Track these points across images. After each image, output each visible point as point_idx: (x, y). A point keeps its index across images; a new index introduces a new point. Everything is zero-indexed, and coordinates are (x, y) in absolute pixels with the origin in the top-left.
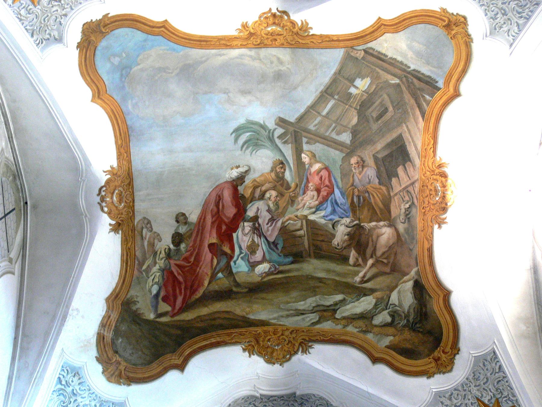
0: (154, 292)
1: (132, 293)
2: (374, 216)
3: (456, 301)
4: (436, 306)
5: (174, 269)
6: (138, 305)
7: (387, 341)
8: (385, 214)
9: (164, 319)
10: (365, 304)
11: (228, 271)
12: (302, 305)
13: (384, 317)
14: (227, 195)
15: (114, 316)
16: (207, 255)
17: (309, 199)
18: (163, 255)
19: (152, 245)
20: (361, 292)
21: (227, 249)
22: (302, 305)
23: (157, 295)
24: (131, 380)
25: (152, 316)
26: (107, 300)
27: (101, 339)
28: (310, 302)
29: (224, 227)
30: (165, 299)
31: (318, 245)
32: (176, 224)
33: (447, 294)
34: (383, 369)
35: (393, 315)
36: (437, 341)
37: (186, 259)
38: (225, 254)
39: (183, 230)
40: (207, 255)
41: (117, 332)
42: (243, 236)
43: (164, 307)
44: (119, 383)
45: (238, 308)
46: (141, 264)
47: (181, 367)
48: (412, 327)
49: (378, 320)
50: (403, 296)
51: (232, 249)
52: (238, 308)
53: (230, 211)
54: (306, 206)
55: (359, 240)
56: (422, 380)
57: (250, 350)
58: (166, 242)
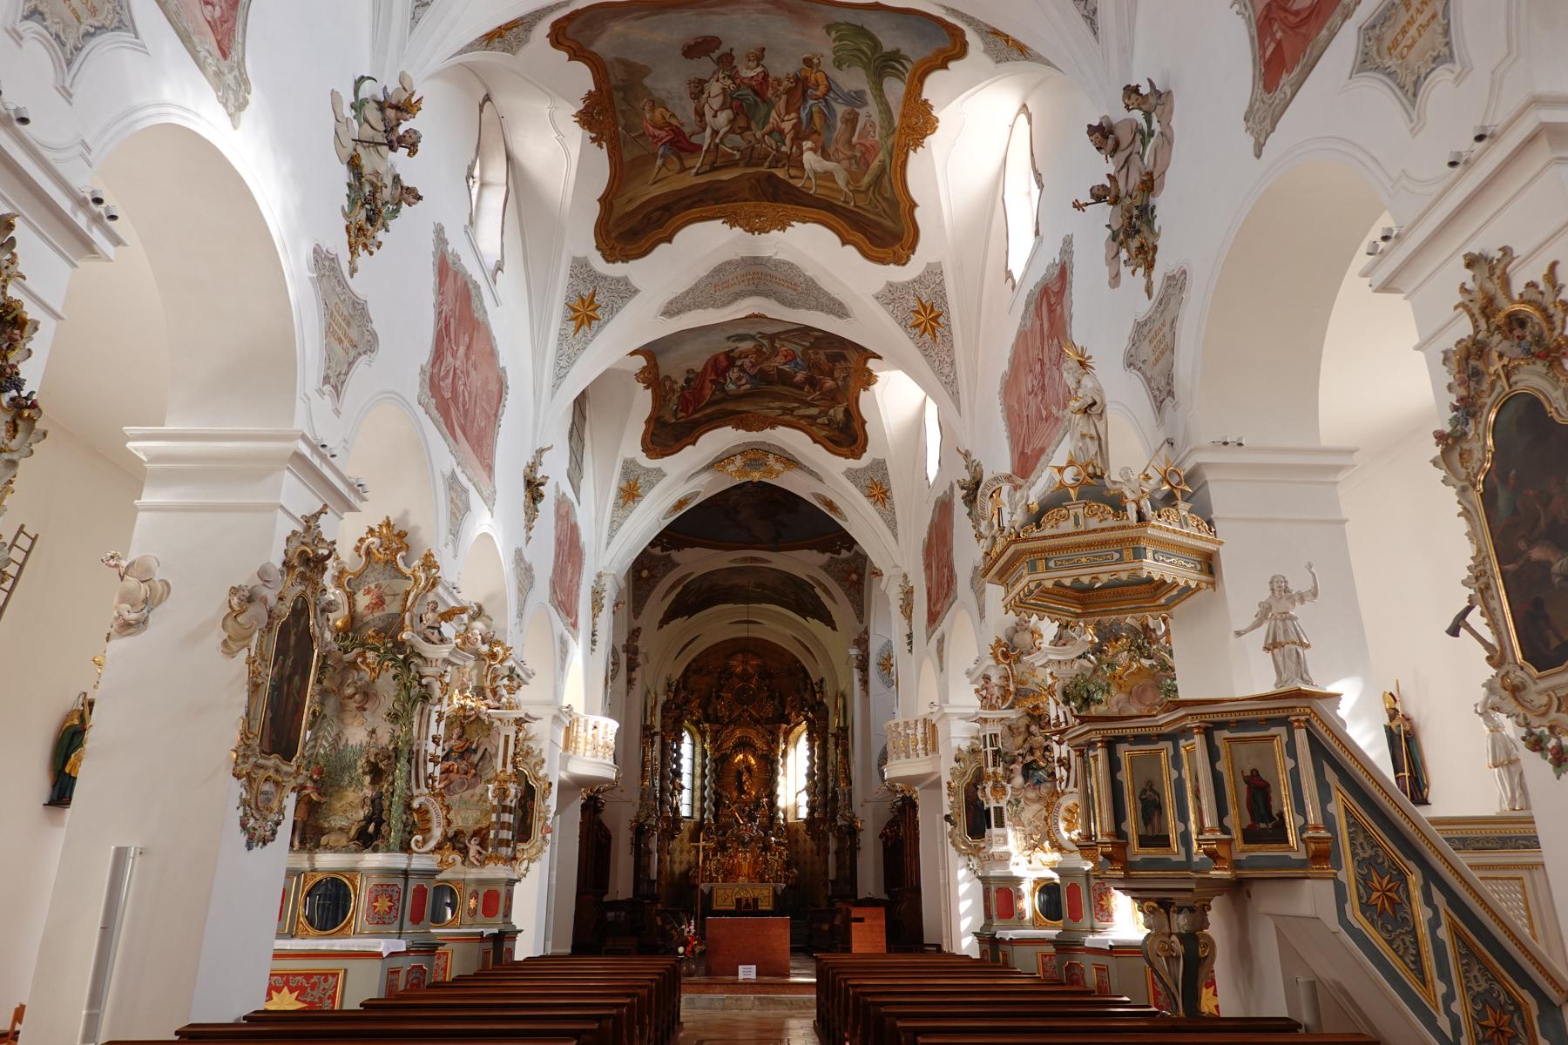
2: (822, 373)
3: (867, 427)
4: (856, 425)
8: (831, 374)
10: (813, 411)
13: (824, 420)
14: (722, 358)
16: (708, 384)
20: (810, 405)
24: (663, 456)
28: (777, 404)
31: (784, 378)
33: (864, 422)
34: (818, 446)
36: (855, 442)
40: (708, 384)
42: (734, 374)
45: (730, 406)
48: (841, 430)
50: (838, 413)
52: (730, 406)
53: (724, 364)
54: (778, 362)
55: (812, 382)
58: (681, 382)
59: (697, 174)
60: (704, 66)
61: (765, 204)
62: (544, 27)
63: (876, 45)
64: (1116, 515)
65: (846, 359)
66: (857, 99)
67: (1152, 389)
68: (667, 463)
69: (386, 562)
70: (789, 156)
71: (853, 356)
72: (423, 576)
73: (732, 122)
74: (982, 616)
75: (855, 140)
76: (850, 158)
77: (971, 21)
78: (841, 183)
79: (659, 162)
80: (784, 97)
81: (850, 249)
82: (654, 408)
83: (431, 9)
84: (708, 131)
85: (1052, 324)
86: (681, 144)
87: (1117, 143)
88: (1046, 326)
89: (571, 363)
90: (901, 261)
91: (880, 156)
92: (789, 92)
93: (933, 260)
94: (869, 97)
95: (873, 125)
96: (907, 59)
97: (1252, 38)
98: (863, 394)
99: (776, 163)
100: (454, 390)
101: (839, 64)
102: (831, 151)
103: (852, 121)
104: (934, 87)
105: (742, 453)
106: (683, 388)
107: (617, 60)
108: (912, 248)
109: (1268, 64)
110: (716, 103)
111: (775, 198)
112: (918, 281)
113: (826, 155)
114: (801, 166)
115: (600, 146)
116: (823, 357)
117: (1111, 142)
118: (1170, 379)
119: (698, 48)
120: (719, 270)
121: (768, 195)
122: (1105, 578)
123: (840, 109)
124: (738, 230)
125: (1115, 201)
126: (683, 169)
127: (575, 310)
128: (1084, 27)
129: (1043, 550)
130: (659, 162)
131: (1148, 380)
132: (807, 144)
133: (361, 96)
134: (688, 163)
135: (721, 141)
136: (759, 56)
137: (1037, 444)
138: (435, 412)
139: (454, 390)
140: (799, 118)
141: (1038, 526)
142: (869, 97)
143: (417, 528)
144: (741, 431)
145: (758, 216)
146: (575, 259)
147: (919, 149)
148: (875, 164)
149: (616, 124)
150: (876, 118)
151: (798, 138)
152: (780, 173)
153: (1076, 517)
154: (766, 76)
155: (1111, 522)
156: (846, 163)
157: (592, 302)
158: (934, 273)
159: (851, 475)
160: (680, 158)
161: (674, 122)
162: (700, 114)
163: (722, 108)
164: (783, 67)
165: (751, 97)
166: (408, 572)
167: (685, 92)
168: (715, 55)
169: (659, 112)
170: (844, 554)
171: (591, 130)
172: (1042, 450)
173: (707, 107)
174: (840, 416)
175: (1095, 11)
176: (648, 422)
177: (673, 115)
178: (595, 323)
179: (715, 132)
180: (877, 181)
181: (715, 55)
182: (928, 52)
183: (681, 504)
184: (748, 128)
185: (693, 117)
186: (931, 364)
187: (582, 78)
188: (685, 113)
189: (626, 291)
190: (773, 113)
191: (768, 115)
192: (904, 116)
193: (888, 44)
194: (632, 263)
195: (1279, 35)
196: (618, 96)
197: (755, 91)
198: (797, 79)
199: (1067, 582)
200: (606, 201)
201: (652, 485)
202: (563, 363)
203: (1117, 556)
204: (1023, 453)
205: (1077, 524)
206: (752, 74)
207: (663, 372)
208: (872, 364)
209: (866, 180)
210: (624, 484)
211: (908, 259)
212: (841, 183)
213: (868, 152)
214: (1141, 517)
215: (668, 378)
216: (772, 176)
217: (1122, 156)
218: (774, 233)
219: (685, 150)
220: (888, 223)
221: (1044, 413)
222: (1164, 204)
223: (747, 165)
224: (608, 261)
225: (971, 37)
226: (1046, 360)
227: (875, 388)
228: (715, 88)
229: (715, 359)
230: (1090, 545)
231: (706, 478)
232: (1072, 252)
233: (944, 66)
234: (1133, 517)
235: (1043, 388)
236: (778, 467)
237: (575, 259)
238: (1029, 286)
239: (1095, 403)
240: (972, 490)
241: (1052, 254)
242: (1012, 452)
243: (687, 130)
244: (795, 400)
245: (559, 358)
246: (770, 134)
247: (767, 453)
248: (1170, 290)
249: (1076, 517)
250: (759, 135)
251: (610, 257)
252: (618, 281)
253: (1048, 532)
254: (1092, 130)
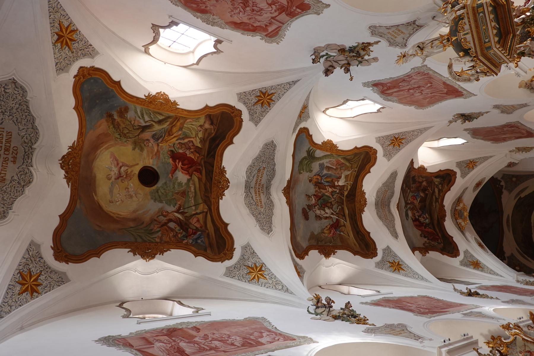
2: (420, 186)
3: (442, 169)
4: (442, 173)
7: (446, 186)
8: (421, 183)
10: (436, 190)
12: (434, 206)
14: (415, 223)
16: (426, 230)
17: (415, 202)
20: (434, 192)
22: (434, 206)
28: (434, 204)
31: (423, 200)
33: (440, 171)
34: (452, 188)
35: (440, 184)
40: (426, 230)
42: (422, 220)
45: (435, 222)
49: (440, 188)
50: (437, 181)
52: (435, 222)
53: (417, 223)
54: (416, 202)
55: (424, 190)
56: (457, 179)
57: (445, 220)
58: (426, 239)
59: (346, 221)
60: (311, 214)
61: (356, 199)
62: (297, 260)
63: (305, 158)
64: (463, 19)
65: (414, 177)
66: (322, 166)
67: (414, 32)
69: (508, 347)
70: (340, 190)
71: (413, 174)
72: (514, 331)
73: (329, 208)
74: (525, 105)
75: (334, 168)
76: (341, 170)
77: (297, 125)
78: (349, 173)
79: (342, 233)
80: (321, 190)
81: (371, 170)
82: (437, 251)
83: (289, 288)
84: (332, 216)
85: (394, 87)
86: (336, 226)
87: (331, 66)
88: (395, 90)
89: (417, 274)
90: (375, 152)
91: (340, 159)
92: (319, 188)
93: (375, 140)
94: (321, 162)
95: (330, 161)
96: (309, 149)
97: (296, 19)
98: (428, 171)
99: (342, 194)
100: (426, 309)
101: (311, 171)
102: (338, 176)
103: (329, 168)
104: (318, 140)
105: (456, 219)
106: (428, 239)
107: (309, 241)
108: (371, 148)
109: (303, 10)
110: (323, 212)
111: (354, 195)
112: (382, 145)
113: (340, 178)
114: (343, 186)
115: (336, 252)
116: (414, 185)
117: (330, 68)
118: (409, 24)
119: (305, 215)
120: (380, 217)
121: (353, 199)
122: (493, 24)
123: (325, 172)
124: (365, 209)
125: (349, 64)
126: (344, 226)
127: (395, 270)
128: (298, 83)
129: (481, 46)
130: (342, 233)
131: (411, 35)
132: (336, 183)
133: (314, 312)
134: (343, 224)
135: (335, 212)
136: (308, 197)
137: (442, 86)
138: (434, 315)
139: (426, 309)
140: (328, 186)
141: (470, 49)
142: (321, 162)
143: (489, 331)
144: (446, 219)
145: (360, 202)
146: (376, 267)
147: (337, 146)
148: (342, 161)
149: (329, 246)
150: (328, 160)
151: (334, 186)
152: (346, 193)
153: (464, 35)
154: (314, 195)
155: (466, 20)
156: (342, 171)
157: (392, 263)
158: (379, 140)
159: (464, 175)
160: (341, 226)
161: (329, 227)
162: (326, 218)
163: (324, 211)
164: (312, 190)
165: (321, 201)
166: (512, 338)
167: (319, 222)
168: (308, 211)
169: (325, 231)
170: (503, 183)
171: (331, 254)
172: (444, 83)
173: (325, 216)
174: (438, 180)
175: (293, 82)
176: (443, 254)
177: (327, 227)
178: (400, 263)
179: (332, 214)
180: (348, 160)
181: (308, 211)
182: (307, 141)
183: (480, 245)
184: (331, 203)
185: (327, 220)
186: (414, 139)
187: (314, 253)
188: (326, 223)
189: (388, 250)
190: (326, 194)
191: (327, 196)
192: (327, 151)
193: (305, 154)
194: (377, 247)
195: (294, 8)
196: (320, 244)
197: (319, 199)
198: (316, 185)
199: (497, 39)
200: (355, 253)
202: (417, 277)
203: (481, 14)
204: (446, 93)
205: (467, 33)
206: (314, 199)
207: (422, 246)
208: (416, 166)
209: (348, 164)
210: (472, 267)
211: (375, 149)
212: (349, 173)
213: (338, 163)
214: (463, 8)
215: (424, 244)
216: (346, 196)
217: (335, 64)
218: (366, 196)
219: (338, 224)
220: (362, 157)
221: (429, 85)
222: (349, 43)
223: (343, 204)
224: (377, 255)
225: (302, 125)
226: (408, 87)
227: (426, 166)
228: (318, 212)
229: (416, 226)
230: (477, 27)
231: (468, 234)
232: (368, 82)
233: (311, 136)
234: (462, 11)
235: (419, 87)
236: (461, 205)
237: (376, 267)
238: (381, 100)
239: (418, 46)
240: (466, 117)
241: (369, 91)
242: (446, 99)
243: (331, 223)
244: (432, 197)
245: (414, 278)
246: (333, 196)
247: (455, 210)
248: (377, 33)
249: (464, 35)
250: (333, 199)
251: (375, 255)
252: (384, 253)
253: (472, 45)
254: (327, 75)
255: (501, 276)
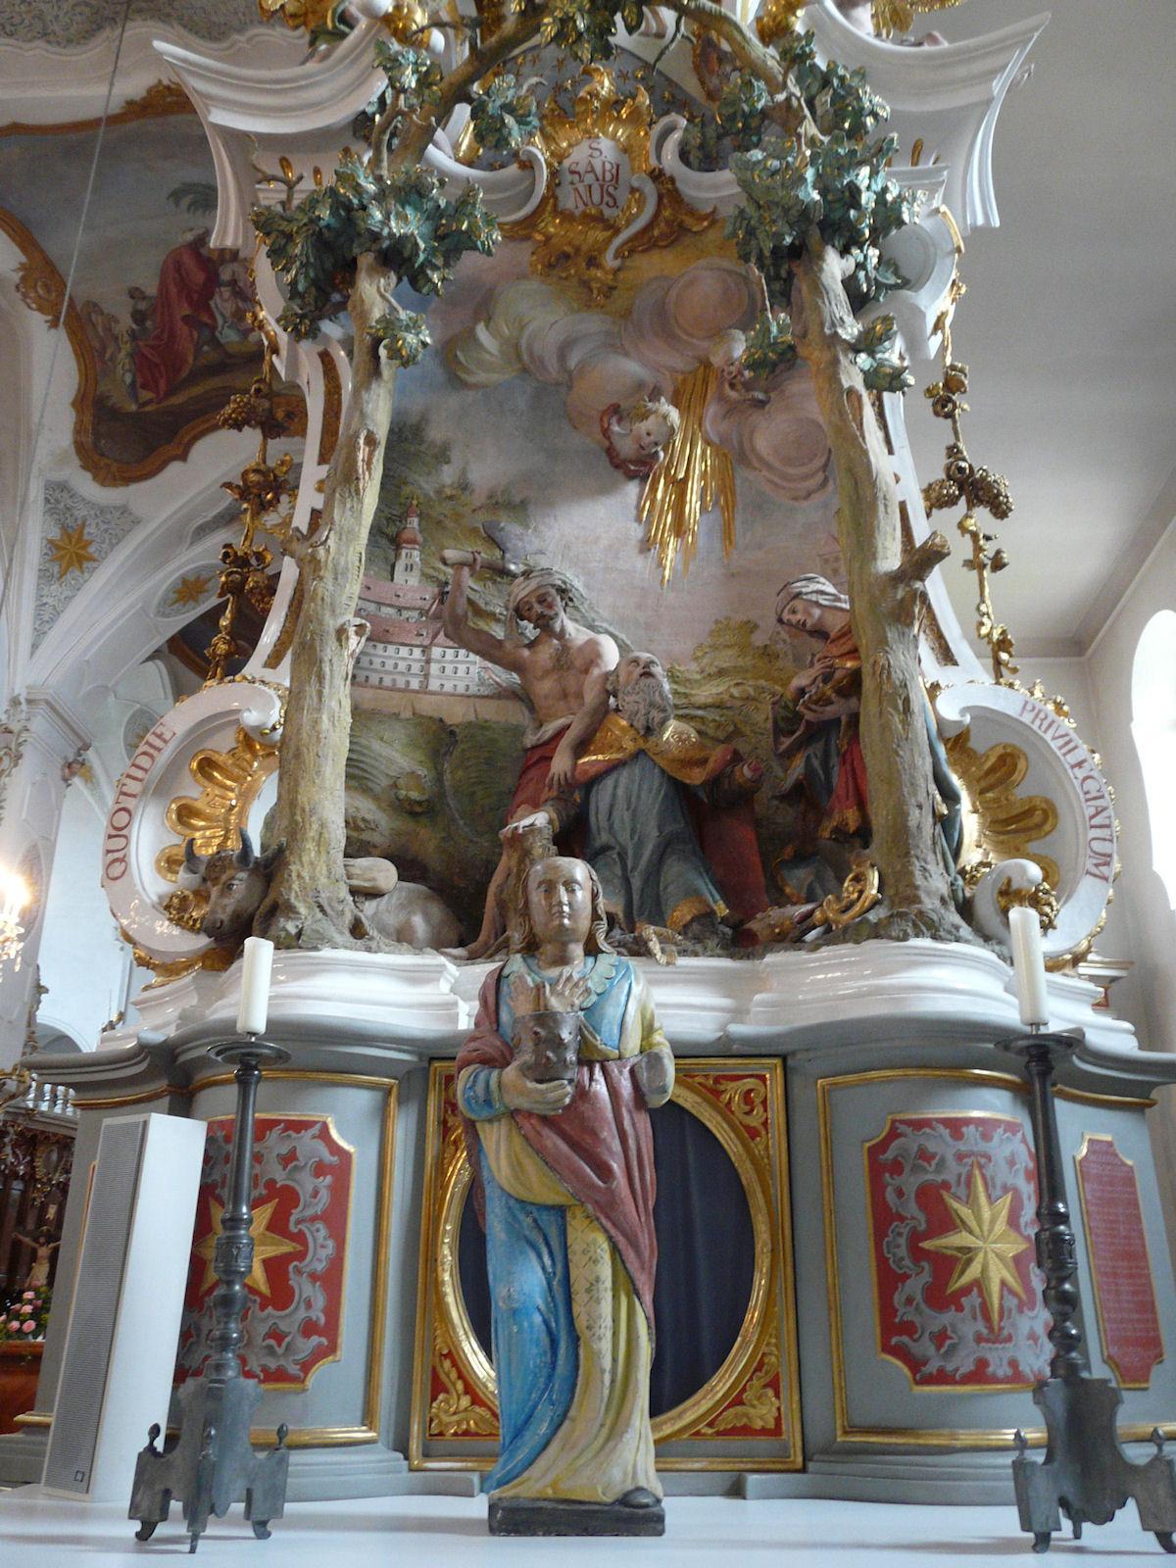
0: (128, 378)
1: (103, 388)
5: (146, 351)
6: (114, 400)
9: (148, 408)
11: (216, 343)
14: (189, 262)
15: (88, 419)
16: (183, 330)
18: (126, 338)
19: (108, 329)
21: (205, 319)
23: (133, 384)
24: (128, 480)
25: (134, 408)
26: (74, 404)
27: (79, 447)
29: (195, 296)
30: (144, 386)
32: (132, 301)
37: (157, 337)
38: (206, 325)
39: (142, 306)
40: (183, 330)
41: (97, 435)
43: (146, 395)
44: (115, 486)
46: (102, 353)
47: (183, 457)
51: (212, 316)
53: (199, 277)
58: (126, 322)
68: (134, 495)
176: (79, 403)
201: (116, 541)
210: (55, 533)
255: (35, 646)
